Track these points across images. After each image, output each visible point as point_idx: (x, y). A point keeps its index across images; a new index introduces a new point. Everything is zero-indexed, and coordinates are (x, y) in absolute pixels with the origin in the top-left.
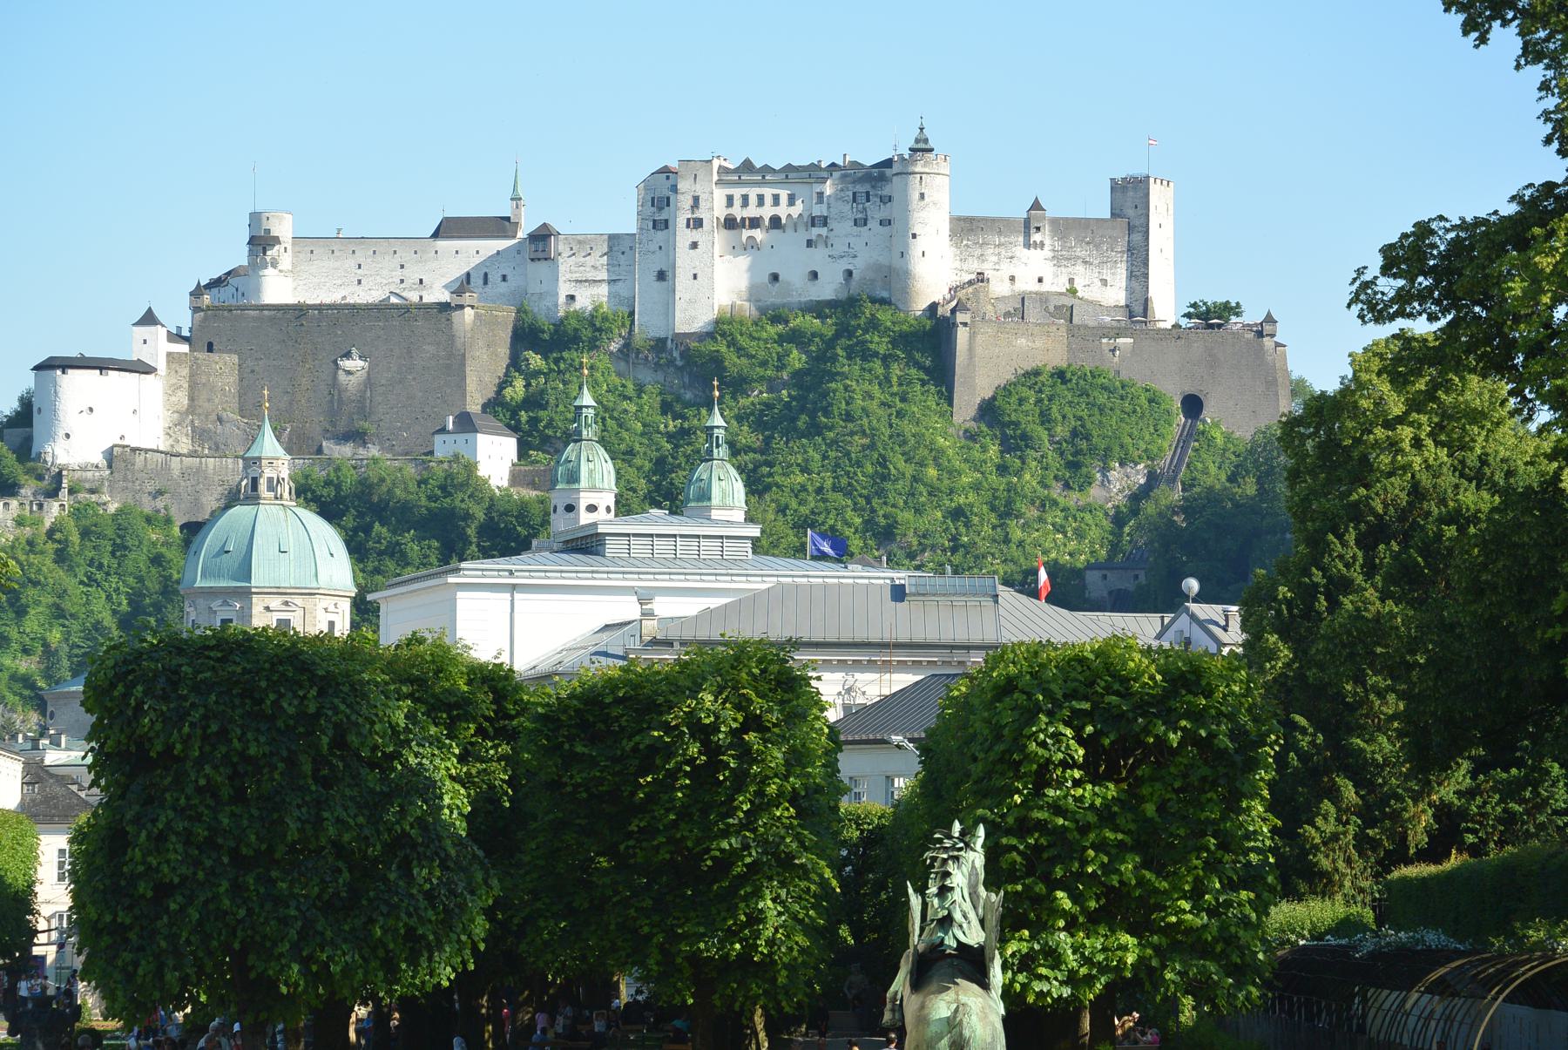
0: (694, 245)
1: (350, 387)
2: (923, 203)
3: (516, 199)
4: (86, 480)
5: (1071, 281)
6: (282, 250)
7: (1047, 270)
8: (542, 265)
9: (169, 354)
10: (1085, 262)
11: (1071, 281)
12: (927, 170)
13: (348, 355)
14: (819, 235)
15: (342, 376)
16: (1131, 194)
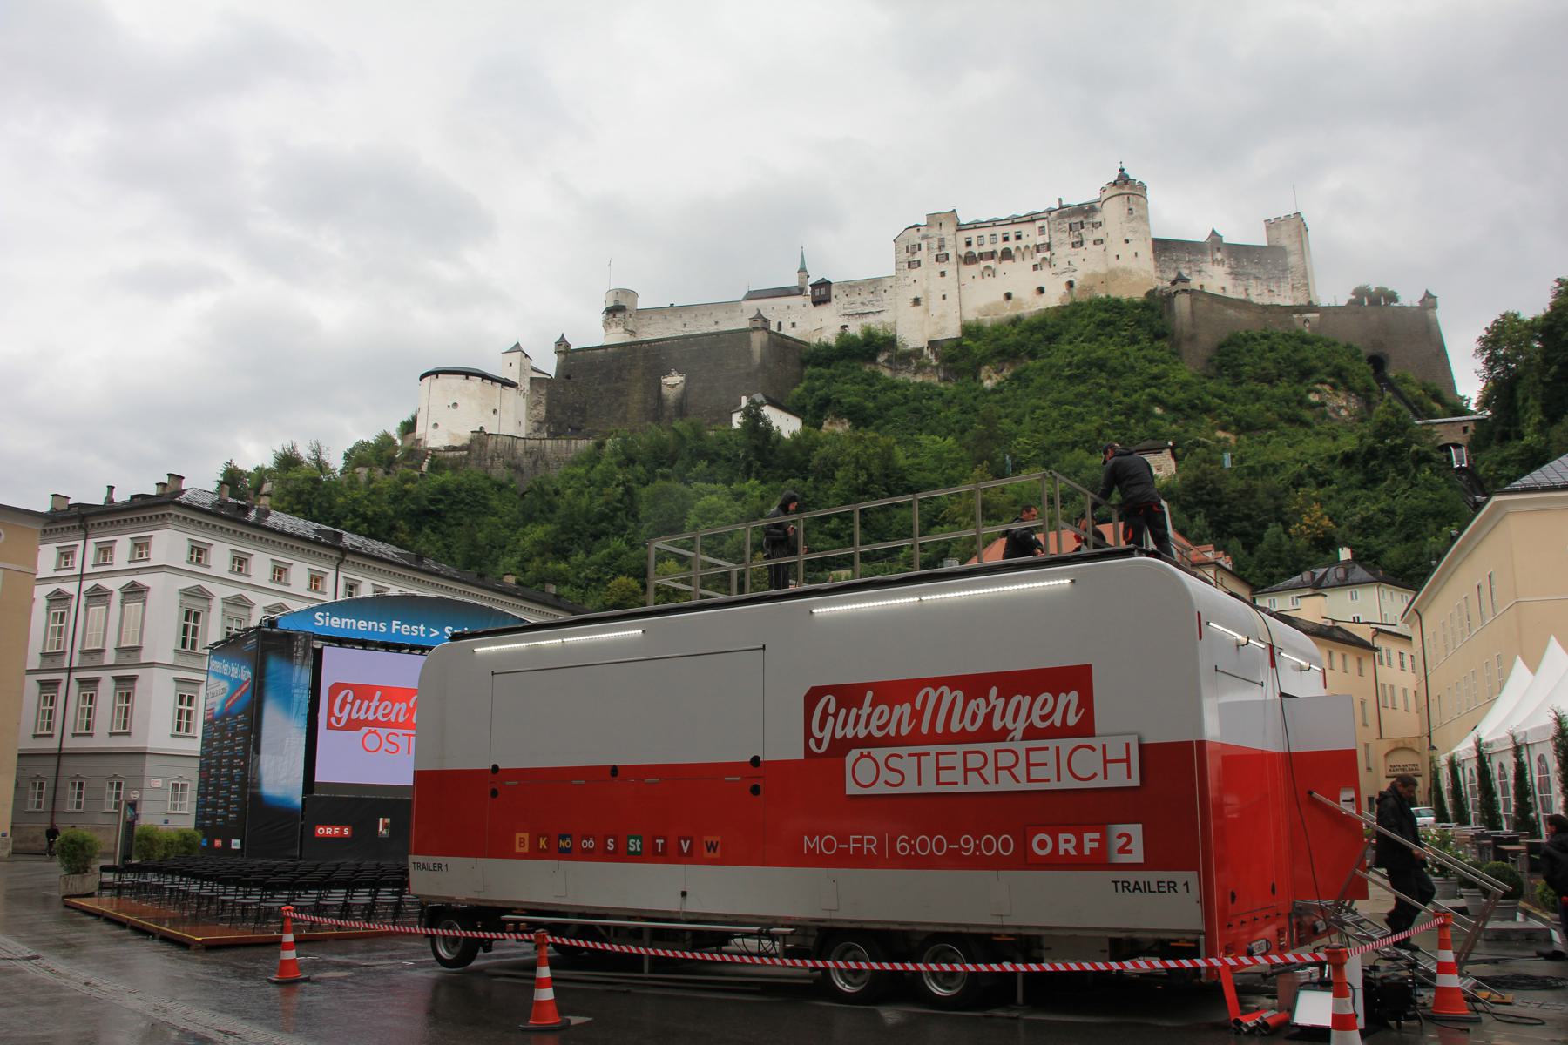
0: (943, 274)
1: (671, 398)
2: (1131, 217)
3: (803, 270)
4: (447, 459)
5: (1246, 290)
6: (627, 316)
7: (1228, 283)
8: (823, 310)
9: (532, 379)
10: (1256, 278)
11: (1246, 290)
12: (1132, 192)
13: (668, 373)
14: (1044, 259)
15: (665, 391)
16: (1284, 228)
